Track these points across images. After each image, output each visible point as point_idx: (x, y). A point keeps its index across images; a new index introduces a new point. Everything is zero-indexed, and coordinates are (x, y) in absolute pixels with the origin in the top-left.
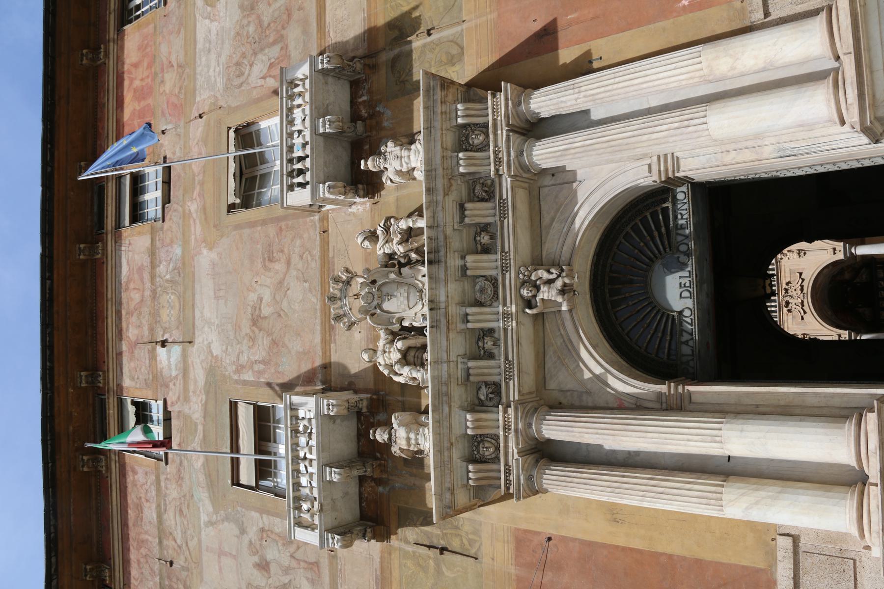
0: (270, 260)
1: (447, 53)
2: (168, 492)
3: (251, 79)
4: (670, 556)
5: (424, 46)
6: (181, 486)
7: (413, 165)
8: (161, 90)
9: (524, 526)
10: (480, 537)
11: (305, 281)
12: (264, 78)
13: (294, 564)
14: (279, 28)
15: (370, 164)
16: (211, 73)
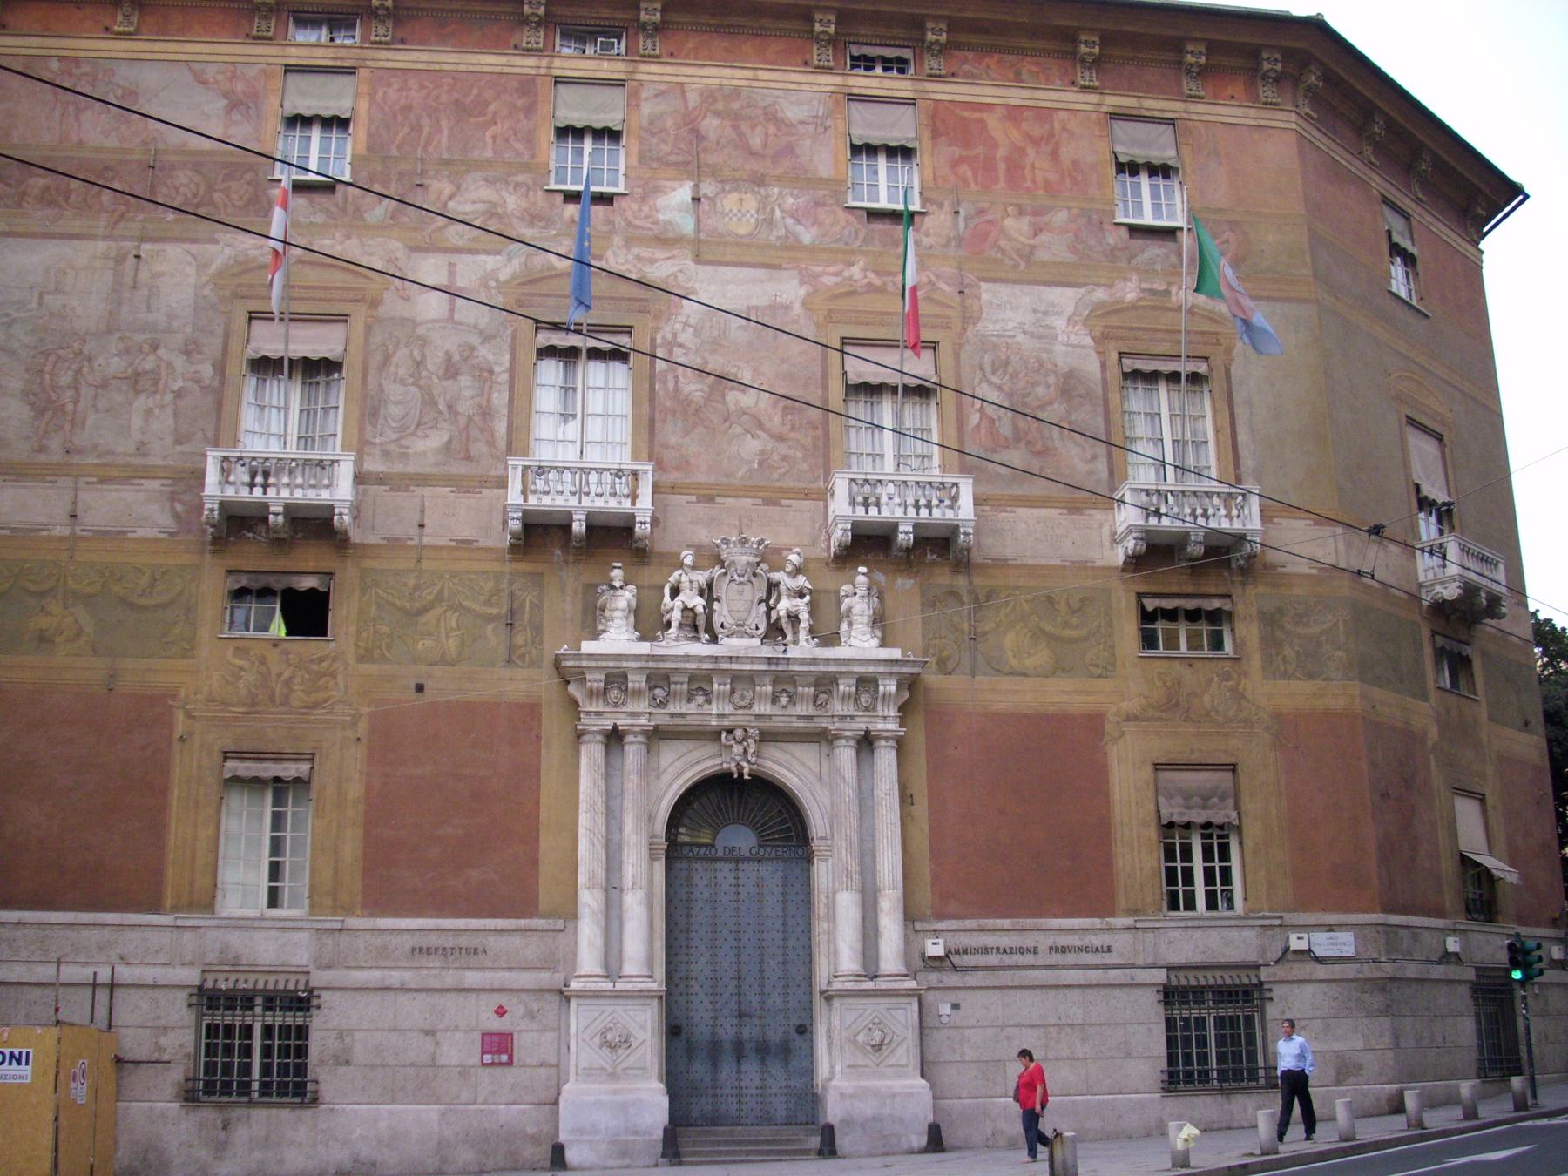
1: (949, 658)
2: (511, 189)
3: (984, 385)
4: (537, 841)
5: (962, 632)
6: (522, 219)
8: (1010, 209)
9: (545, 711)
11: (760, 463)
13: (462, 421)
14: (1030, 437)
16: (1009, 314)
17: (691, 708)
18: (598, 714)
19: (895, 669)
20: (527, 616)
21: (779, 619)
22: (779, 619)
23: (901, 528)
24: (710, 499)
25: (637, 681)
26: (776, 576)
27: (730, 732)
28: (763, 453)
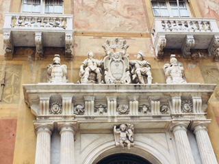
0: (128, 9)
7: (174, 78)
10: (12, 103)
12: (209, 8)
15: (173, 59)
17: (97, 114)
18: (46, 117)
19: (200, 90)
20: (12, 81)
21: (137, 78)
22: (137, 78)
23: (188, 37)
24: (100, 37)
25: (67, 100)
26: (133, 61)
27: (118, 127)
28: (121, 22)
